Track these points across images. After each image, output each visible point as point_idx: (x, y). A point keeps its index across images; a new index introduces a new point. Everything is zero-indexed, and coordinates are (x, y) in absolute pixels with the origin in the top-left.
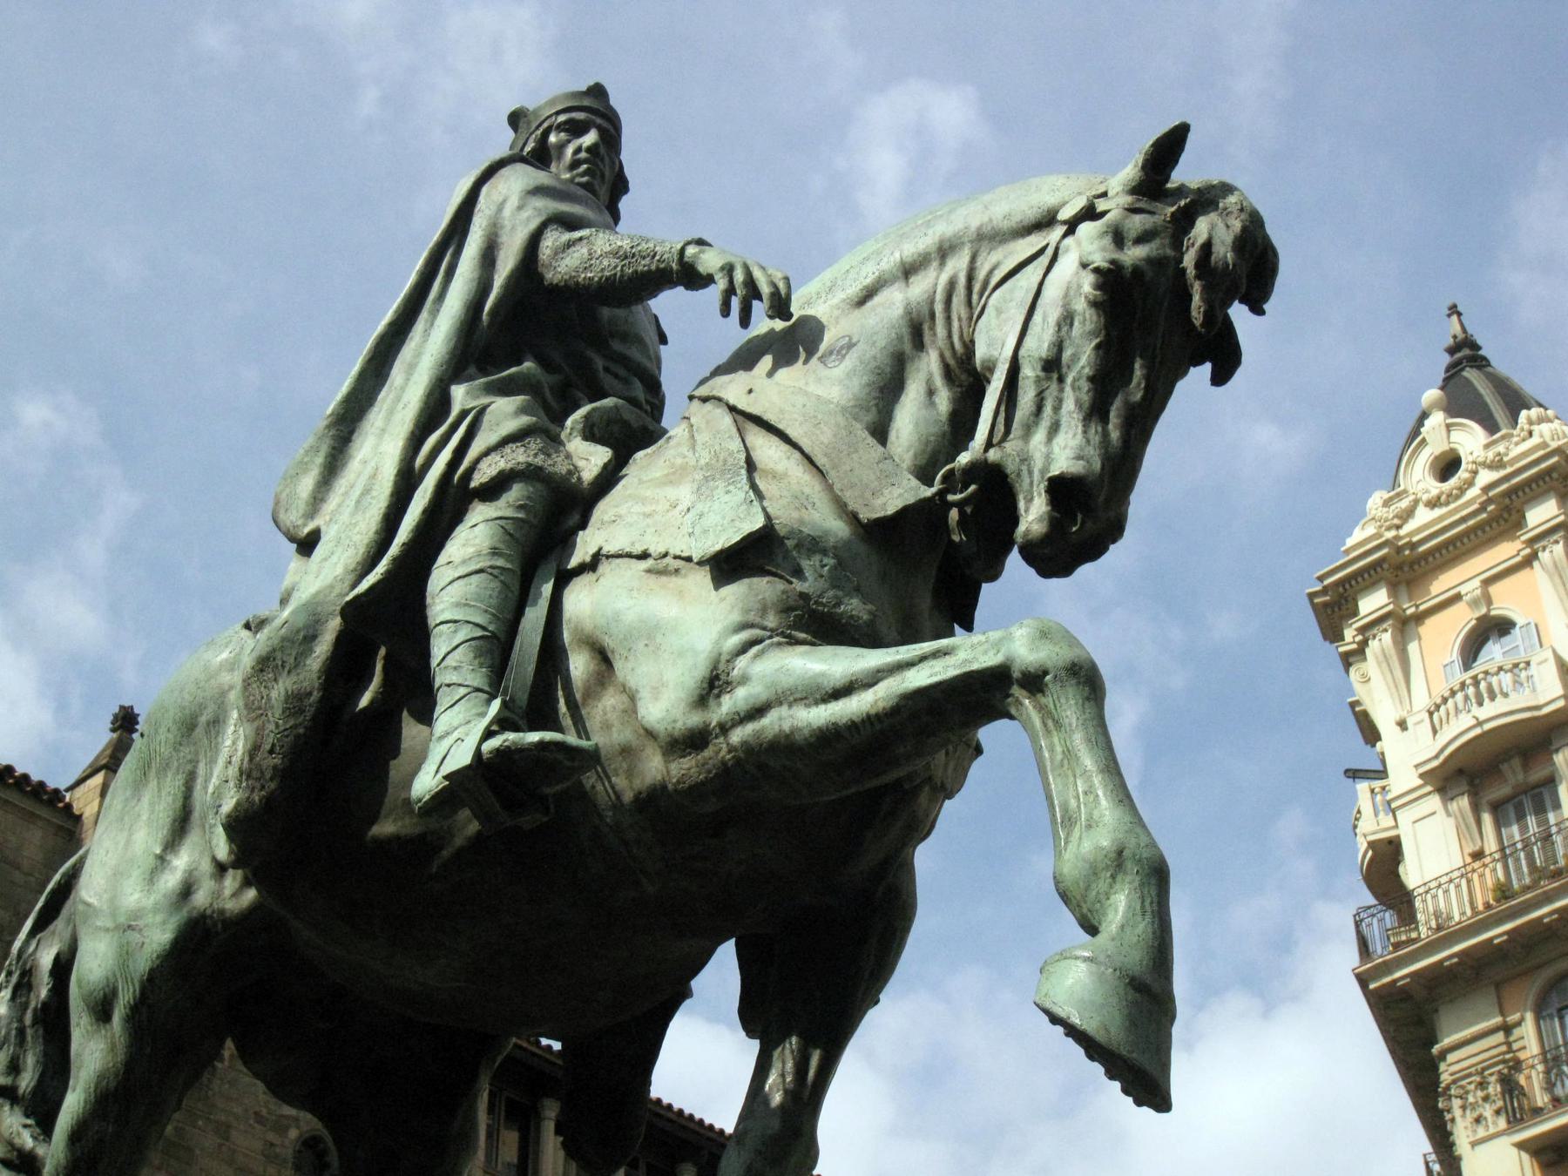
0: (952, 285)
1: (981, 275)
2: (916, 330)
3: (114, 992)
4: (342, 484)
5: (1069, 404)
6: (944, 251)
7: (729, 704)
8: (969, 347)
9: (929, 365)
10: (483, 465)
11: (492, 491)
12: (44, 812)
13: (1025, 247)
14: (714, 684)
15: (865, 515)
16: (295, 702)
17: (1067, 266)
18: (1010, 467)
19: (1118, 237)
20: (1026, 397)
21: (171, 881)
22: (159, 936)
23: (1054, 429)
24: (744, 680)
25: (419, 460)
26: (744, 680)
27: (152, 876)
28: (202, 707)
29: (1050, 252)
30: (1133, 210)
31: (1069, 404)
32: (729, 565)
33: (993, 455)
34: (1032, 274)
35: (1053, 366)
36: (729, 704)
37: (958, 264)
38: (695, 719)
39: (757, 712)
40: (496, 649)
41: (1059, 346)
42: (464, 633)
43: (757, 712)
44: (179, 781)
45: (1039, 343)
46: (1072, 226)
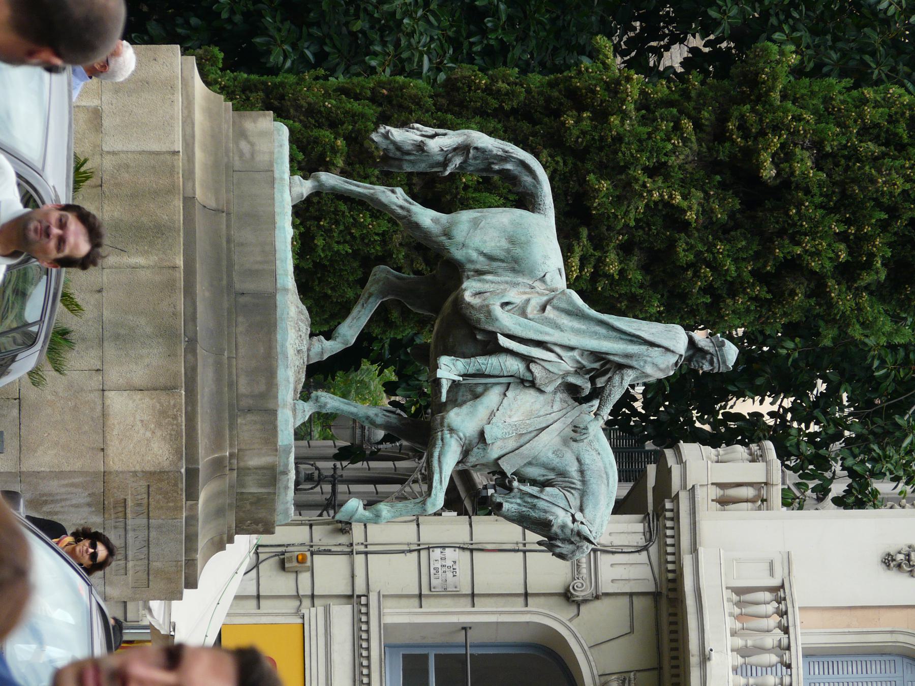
0: (573, 483)
1: (572, 491)
2: (562, 474)
3: (450, 239)
4: (563, 315)
5: (524, 509)
6: (584, 482)
7: (446, 432)
8: (553, 486)
9: (551, 476)
10: (538, 366)
11: (528, 369)
13: (575, 501)
14: (452, 430)
15: (500, 462)
16: (479, 321)
18: (512, 494)
19: (563, 527)
20: (529, 500)
21: (474, 255)
22: (458, 254)
23: (519, 505)
24: (451, 437)
25: (549, 345)
26: (451, 437)
27: (477, 250)
28: (519, 265)
29: (568, 509)
30: (572, 530)
31: (524, 509)
32: (482, 435)
33: (516, 490)
34: (563, 503)
35: (534, 507)
36: (446, 432)
37: (579, 485)
38: (445, 424)
39: (442, 440)
40: (480, 375)
41: (539, 509)
42: (483, 366)
43: (442, 440)
44: (503, 258)
45: (541, 504)
46: (573, 516)
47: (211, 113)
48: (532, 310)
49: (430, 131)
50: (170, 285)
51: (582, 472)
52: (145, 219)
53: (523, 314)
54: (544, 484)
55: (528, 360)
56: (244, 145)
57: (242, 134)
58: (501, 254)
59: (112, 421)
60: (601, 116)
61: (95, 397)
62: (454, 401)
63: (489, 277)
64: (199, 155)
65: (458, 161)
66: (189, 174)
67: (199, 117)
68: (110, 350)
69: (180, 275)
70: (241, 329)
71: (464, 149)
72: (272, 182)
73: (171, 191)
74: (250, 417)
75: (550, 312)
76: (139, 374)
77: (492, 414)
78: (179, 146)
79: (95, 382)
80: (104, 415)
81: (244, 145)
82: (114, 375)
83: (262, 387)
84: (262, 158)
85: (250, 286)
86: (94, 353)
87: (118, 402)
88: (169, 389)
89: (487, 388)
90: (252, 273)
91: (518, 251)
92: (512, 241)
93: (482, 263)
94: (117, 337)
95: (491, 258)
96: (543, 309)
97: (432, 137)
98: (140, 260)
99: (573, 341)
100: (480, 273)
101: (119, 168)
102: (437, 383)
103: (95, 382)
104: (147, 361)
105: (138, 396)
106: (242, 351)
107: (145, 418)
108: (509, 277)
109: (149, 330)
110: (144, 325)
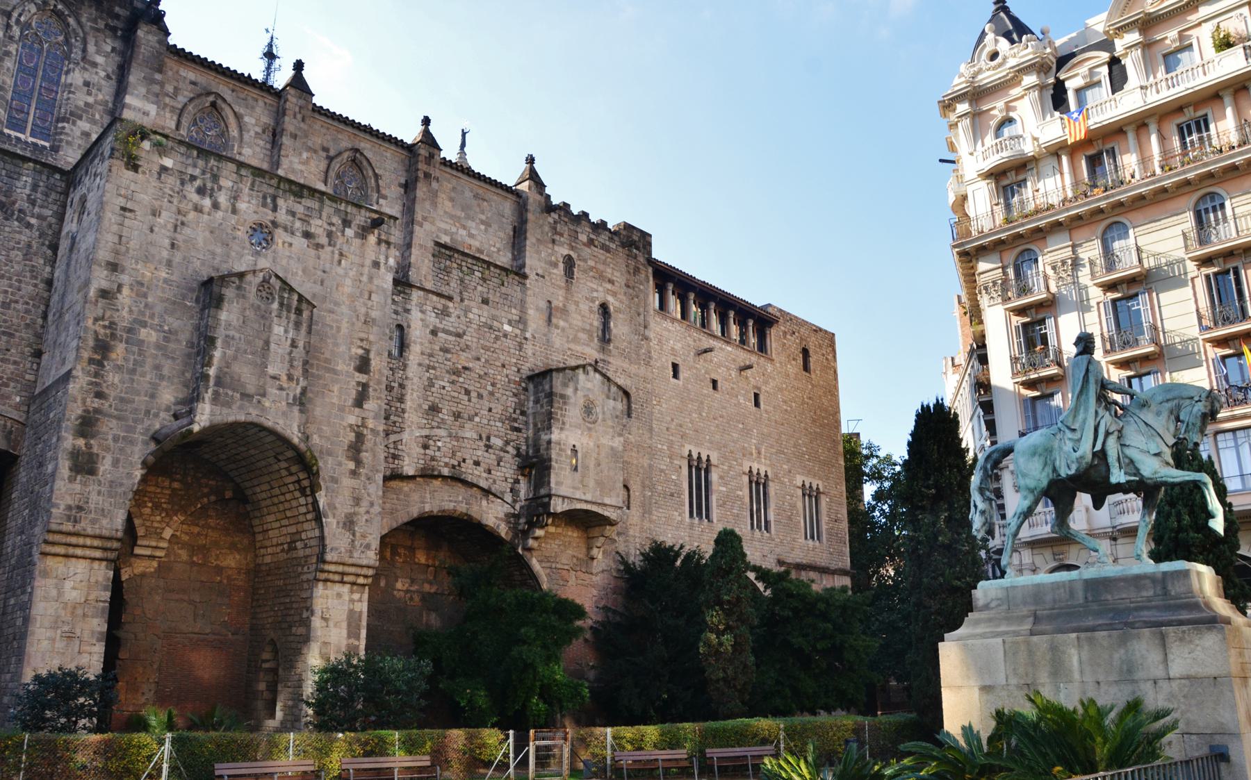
6: (1174, 399)
12: (510, 196)
13: (1188, 402)
17: (1196, 409)
21: (1044, 474)
22: (1045, 483)
34: (1189, 408)
37: (1176, 401)
47: (977, 623)
48: (1076, 436)
49: (973, 509)
50: (1091, 641)
51: (1168, 401)
52: (1048, 657)
53: (1079, 440)
54: (1178, 419)
55: (1107, 434)
56: (993, 605)
57: (987, 607)
58: (1042, 459)
59: (1192, 672)
60: (919, 542)
61: (1175, 684)
62: (1137, 472)
63: (1057, 463)
64: (1003, 628)
65: (988, 493)
66: (1016, 634)
67: (979, 630)
68: (1139, 675)
69: (1083, 635)
70: (1109, 597)
71: (981, 491)
72: (1014, 587)
73: (1028, 643)
74: (1170, 588)
75: (1076, 426)
76: (1154, 656)
77: (1142, 451)
78: (999, 640)
79: (1164, 684)
80: (1188, 678)
81: (993, 605)
82: (1159, 672)
83: (1147, 582)
84: (1000, 594)
85: (1080, 595)
86: (1142, 686)
87: (1176, 669)
88: (1163, 638)
89: (1127, 457)
90: (1072, 593)
91: (1040, 450)
92: (1034, 454)
93: (1049, 470)
94: (1130, 671)
95: (1045, 464)
96: (1074, 430)
97: (976, 506)
98: (1075, 660)
99: (1092, 411)
100: (1054, 470)
101: (1016, 674)
102: (1128, 482)
103: (1164, 684)
104: (1144, 652)
105: (1170, 657)
106: (1124, 596)
107: (1186, 651)
108: (1056, 454)
109: (1122, 651)
110: (1119, 655)
